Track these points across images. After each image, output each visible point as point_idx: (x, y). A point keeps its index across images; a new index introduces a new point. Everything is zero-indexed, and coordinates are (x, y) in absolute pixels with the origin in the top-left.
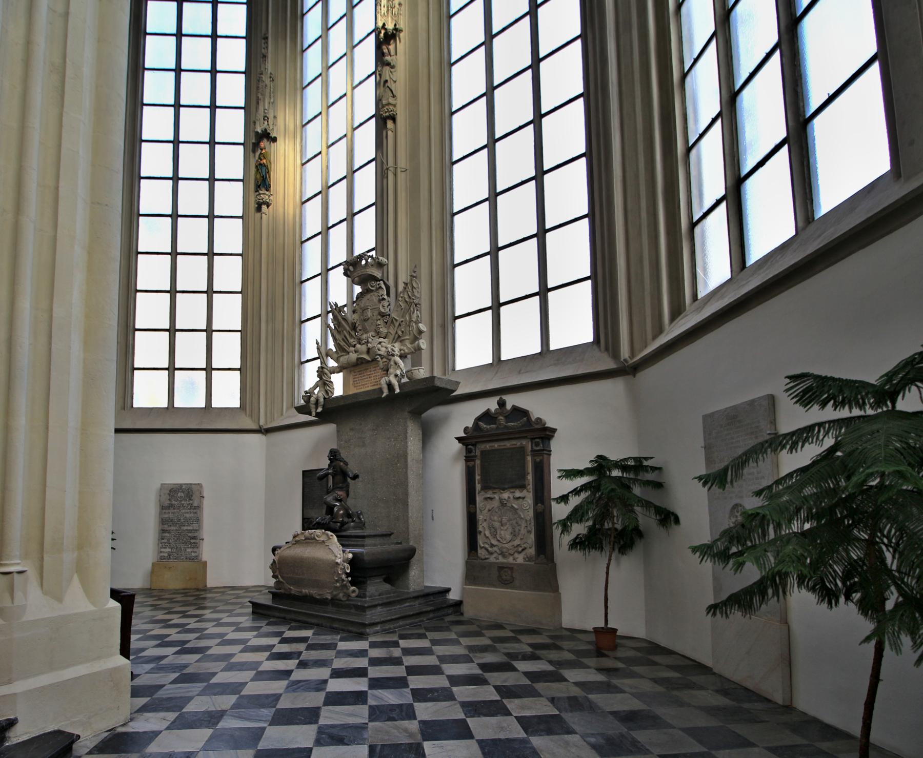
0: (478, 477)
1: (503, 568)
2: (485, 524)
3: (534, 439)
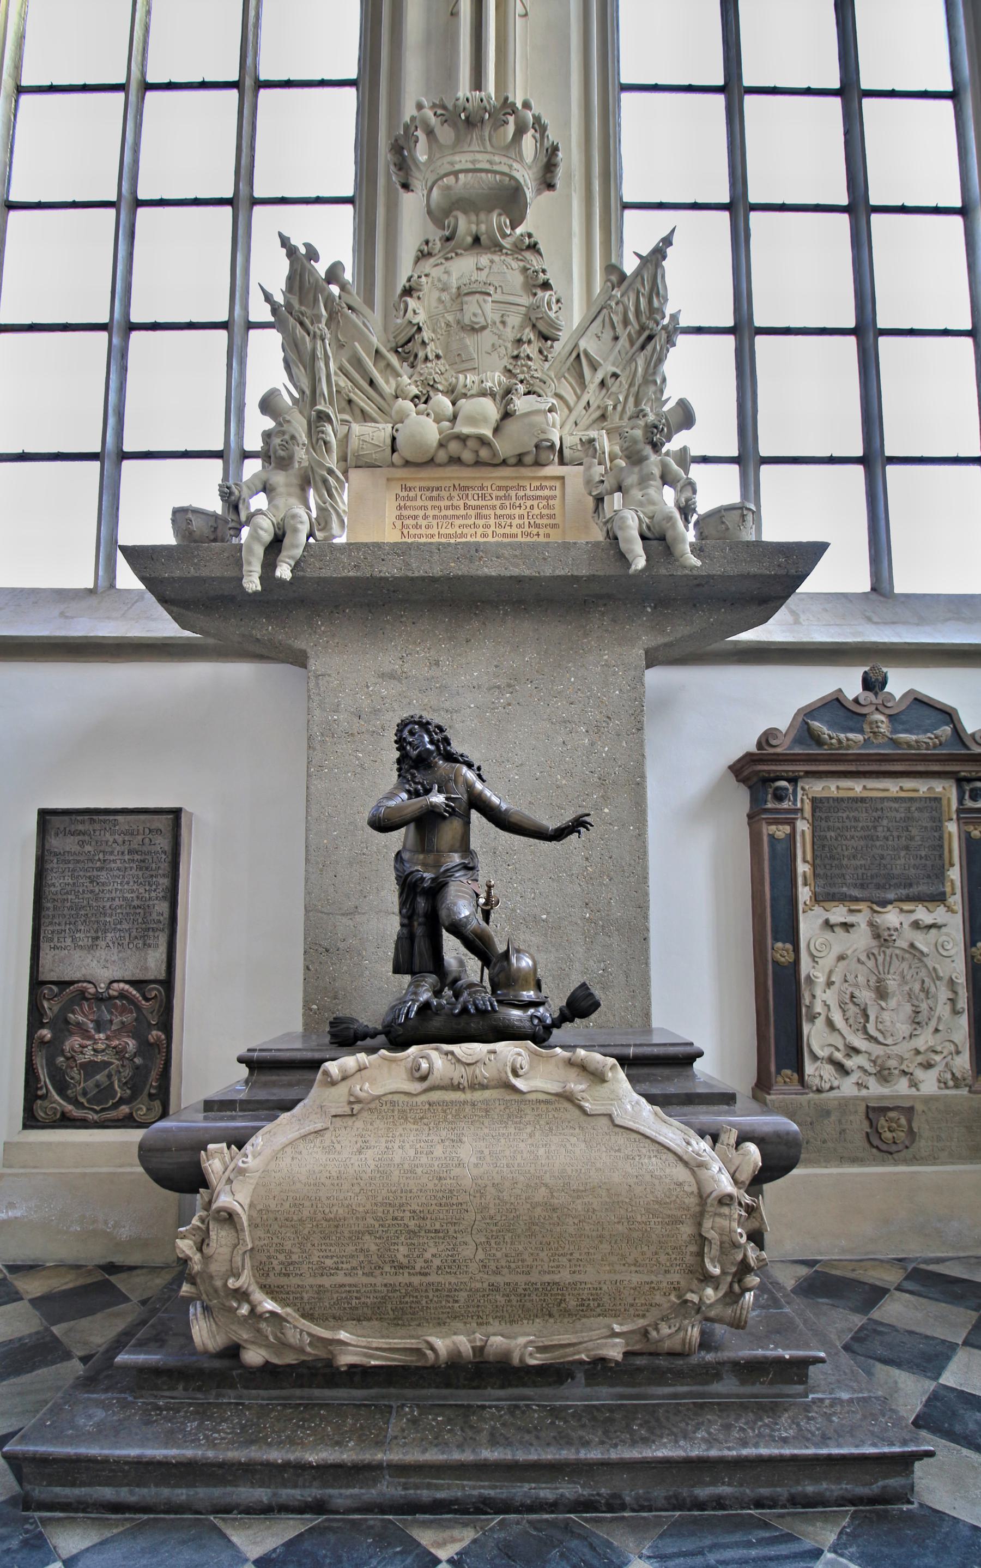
0: (802, 868)
1: (884, 1110)
2: (830, 996)
3: (969, 780)
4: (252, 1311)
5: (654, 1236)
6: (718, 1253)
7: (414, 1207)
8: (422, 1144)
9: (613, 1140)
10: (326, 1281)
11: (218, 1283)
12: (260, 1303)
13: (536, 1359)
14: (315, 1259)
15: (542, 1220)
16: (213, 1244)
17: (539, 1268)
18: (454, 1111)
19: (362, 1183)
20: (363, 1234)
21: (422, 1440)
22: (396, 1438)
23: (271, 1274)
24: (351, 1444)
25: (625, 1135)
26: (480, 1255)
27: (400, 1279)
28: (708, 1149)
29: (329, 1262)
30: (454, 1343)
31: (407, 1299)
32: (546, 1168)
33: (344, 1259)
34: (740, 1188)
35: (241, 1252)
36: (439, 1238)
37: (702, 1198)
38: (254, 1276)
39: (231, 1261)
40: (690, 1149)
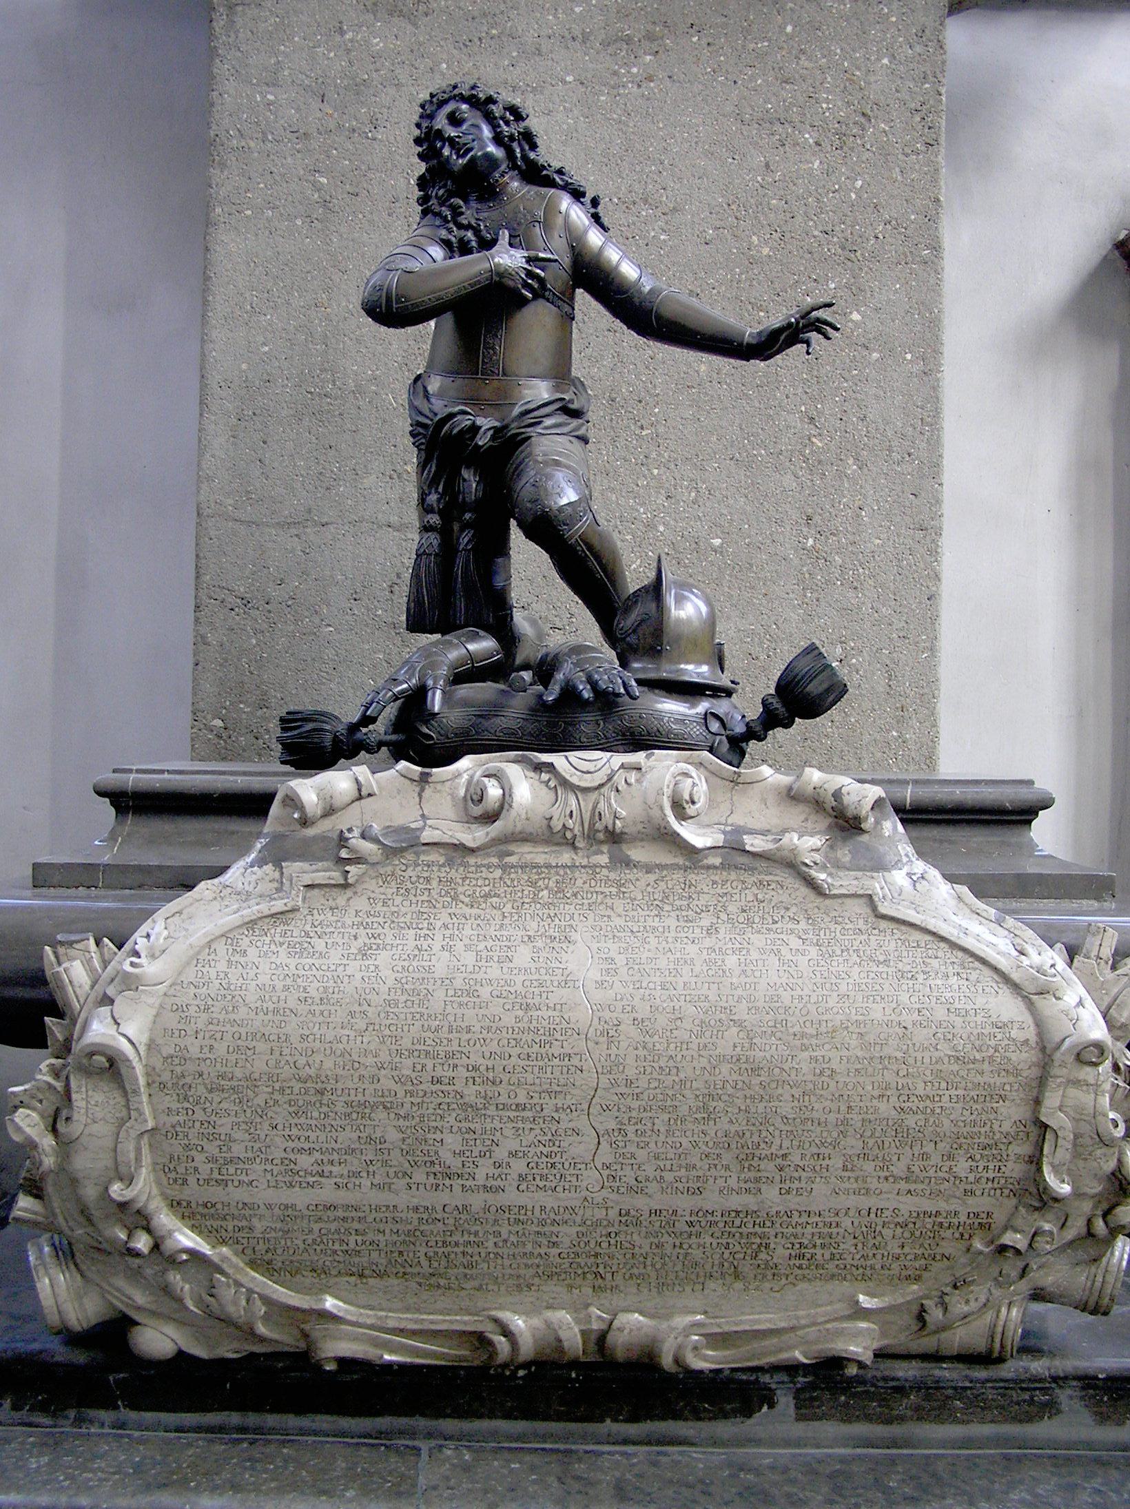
4: (156, 1247)
5: (946, 1122)
6: (1068, 1156)
7: (475, 1059)
8: (490, 943)
9: (873, 943)
10: (300, 1198)
11: (90, 1192)
12: (170, 1233)
13: (705, 1358)
14: (278, 1154)
15: (730, 1091)
16: (79, 1116)
17: (720, 1182)
18: (552, 884)
19: (371, 1012)
20: (374, 1107)
21: (486, 1492)
22: (435, 1488)
23: (192, 1180)
24: (350, 1494)
25: (898, 934)
26: (605, 1155)
27: (444, 1197)
28: (1061, 965)
29: (305, 1161)
30: (548, 1324)
31: (457, 1237)
32: (739, 992)
33: (335, 1157)
34: (1117, 1039)
35: (133, 1134)
36: (523, 1120)
37: (1046, 1051)
38: (159, 1183)
39: (115, 1150)
40: (1025, 961)
